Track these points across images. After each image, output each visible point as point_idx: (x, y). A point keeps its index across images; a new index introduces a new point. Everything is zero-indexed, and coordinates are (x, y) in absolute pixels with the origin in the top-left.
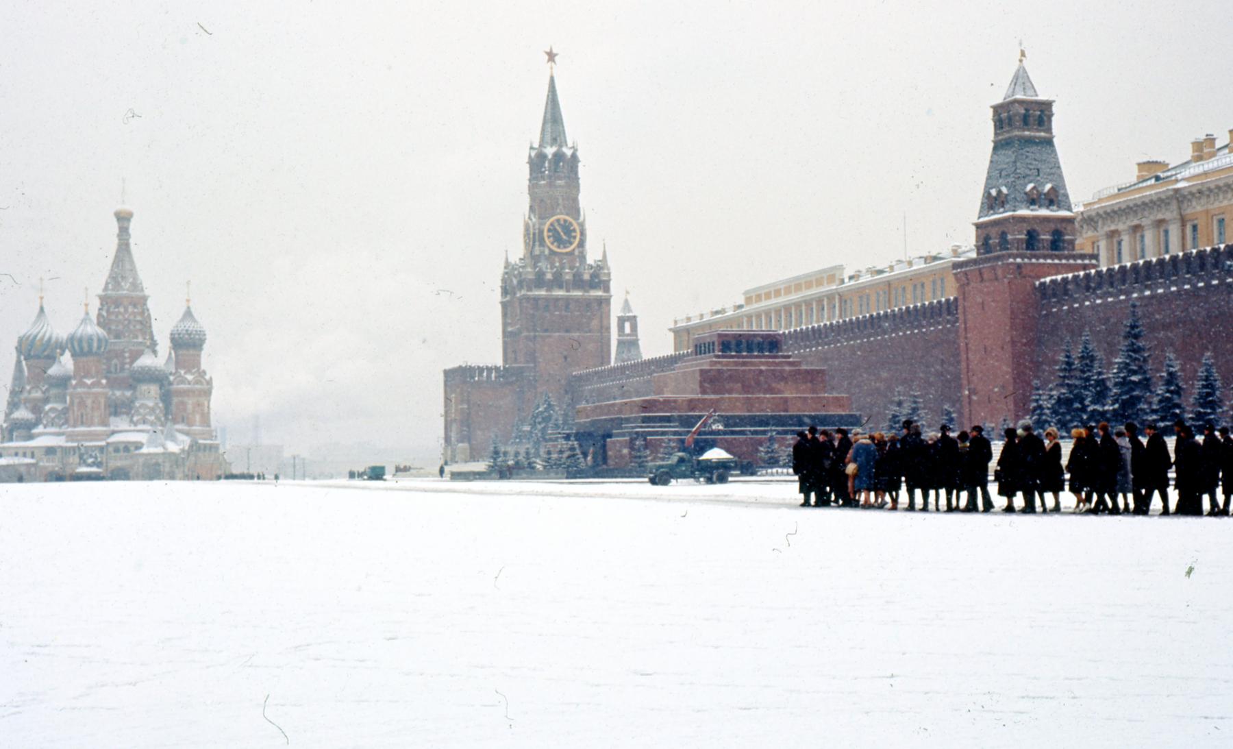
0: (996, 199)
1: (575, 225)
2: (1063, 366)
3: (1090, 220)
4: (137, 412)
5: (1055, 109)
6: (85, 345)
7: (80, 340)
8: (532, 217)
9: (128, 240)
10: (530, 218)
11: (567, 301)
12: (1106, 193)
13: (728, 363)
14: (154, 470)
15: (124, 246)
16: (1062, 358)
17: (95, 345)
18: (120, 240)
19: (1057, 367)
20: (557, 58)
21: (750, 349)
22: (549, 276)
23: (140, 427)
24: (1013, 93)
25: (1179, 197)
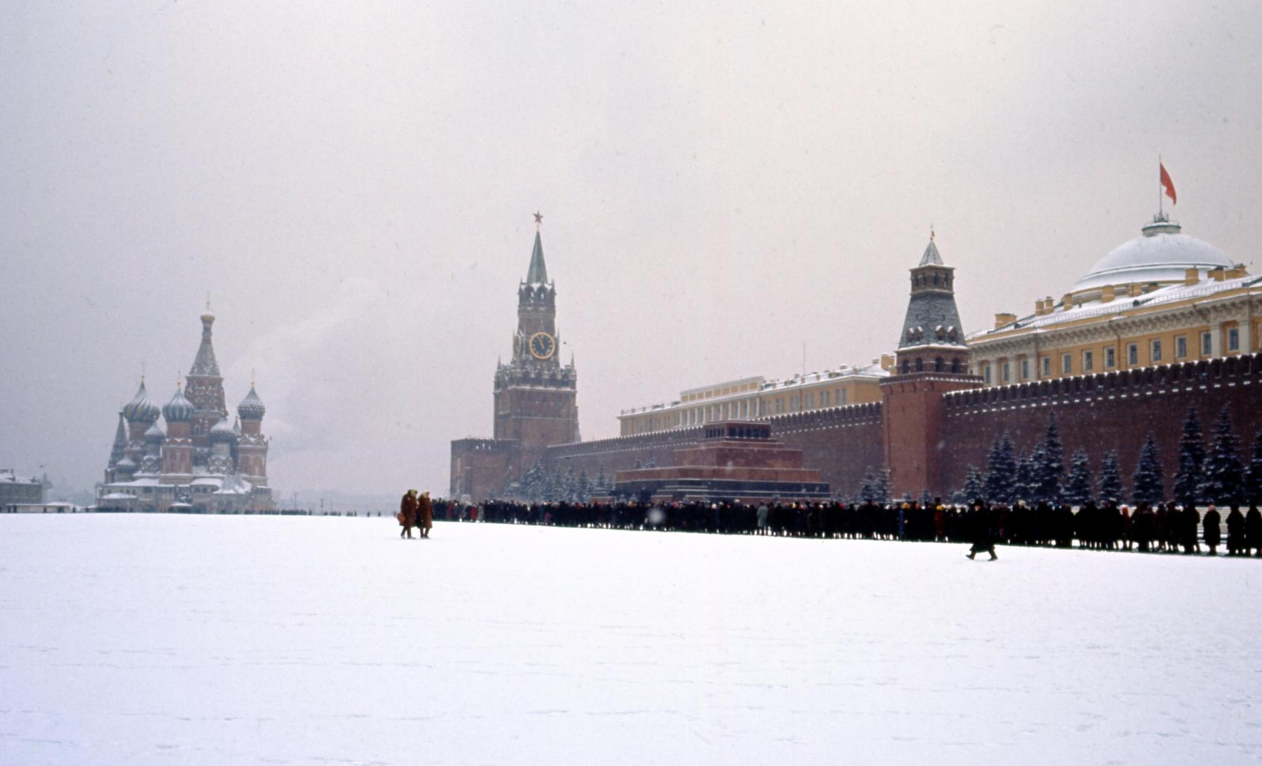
0: (913, 335)
1: (553, 340)
2: (994, 455)
5: (955, 273)
6: (177, 414)
7: (174, 409)
8: (521, 333)
10: (518, 333)
13: (735, 443)
14: (227, 507)
15: (207, 340)
16: (992, 449)
17: (185, 413)
19: (989, 456)
20: (542, 220)
22: (533, 376)
23: (215, 475)
24: (927, 262)
25: (1037, 339)
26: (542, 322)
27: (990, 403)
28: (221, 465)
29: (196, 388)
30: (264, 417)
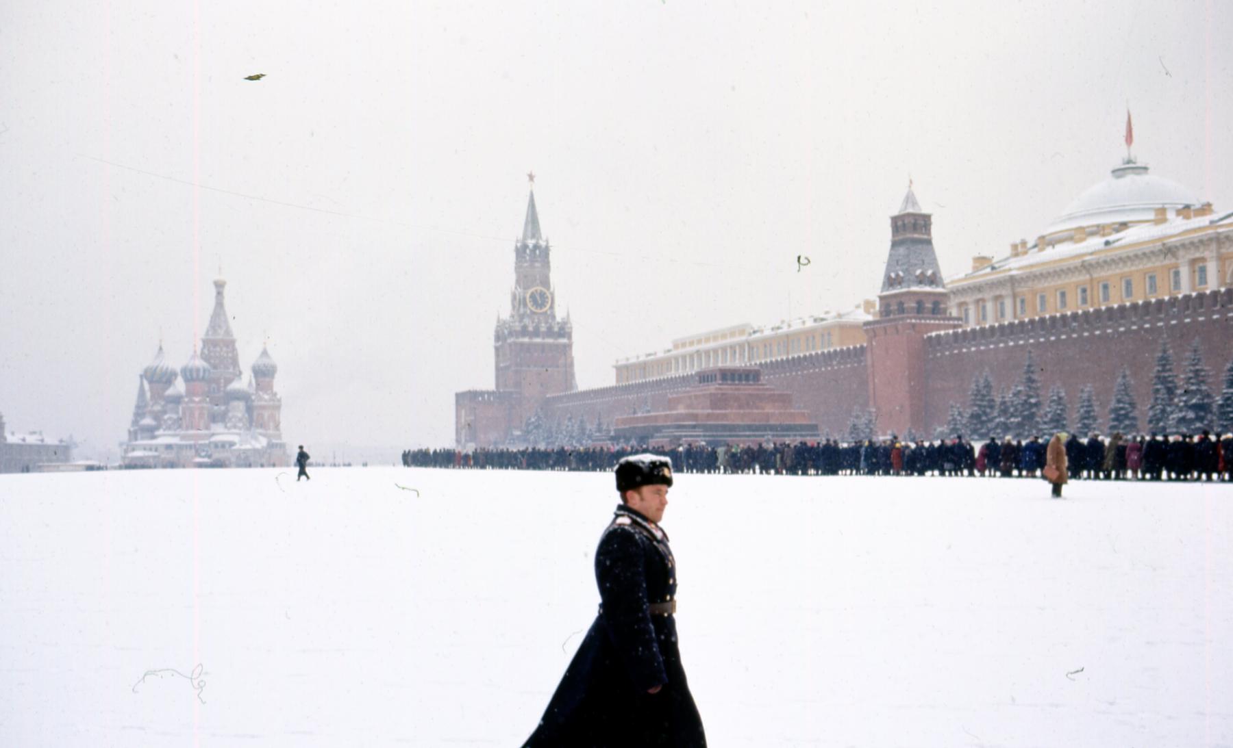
0: (894, 279)
1: (550, 296)
3: (957, 292)
4: (230, 419)
5: (933, 219)
7: (191, 371)
8: (518, 287)
10: (516, 288)
12: (956, 277)
13: (728, 388)
14: (246, 461)
15: (220, 304)
16: (973, 386)
17: (201, 374)
20: (535, 179)
22: (531, 329)
24: (906, 208)
25: (1012, 280)
26: (538, 277)
27: (969, 343)
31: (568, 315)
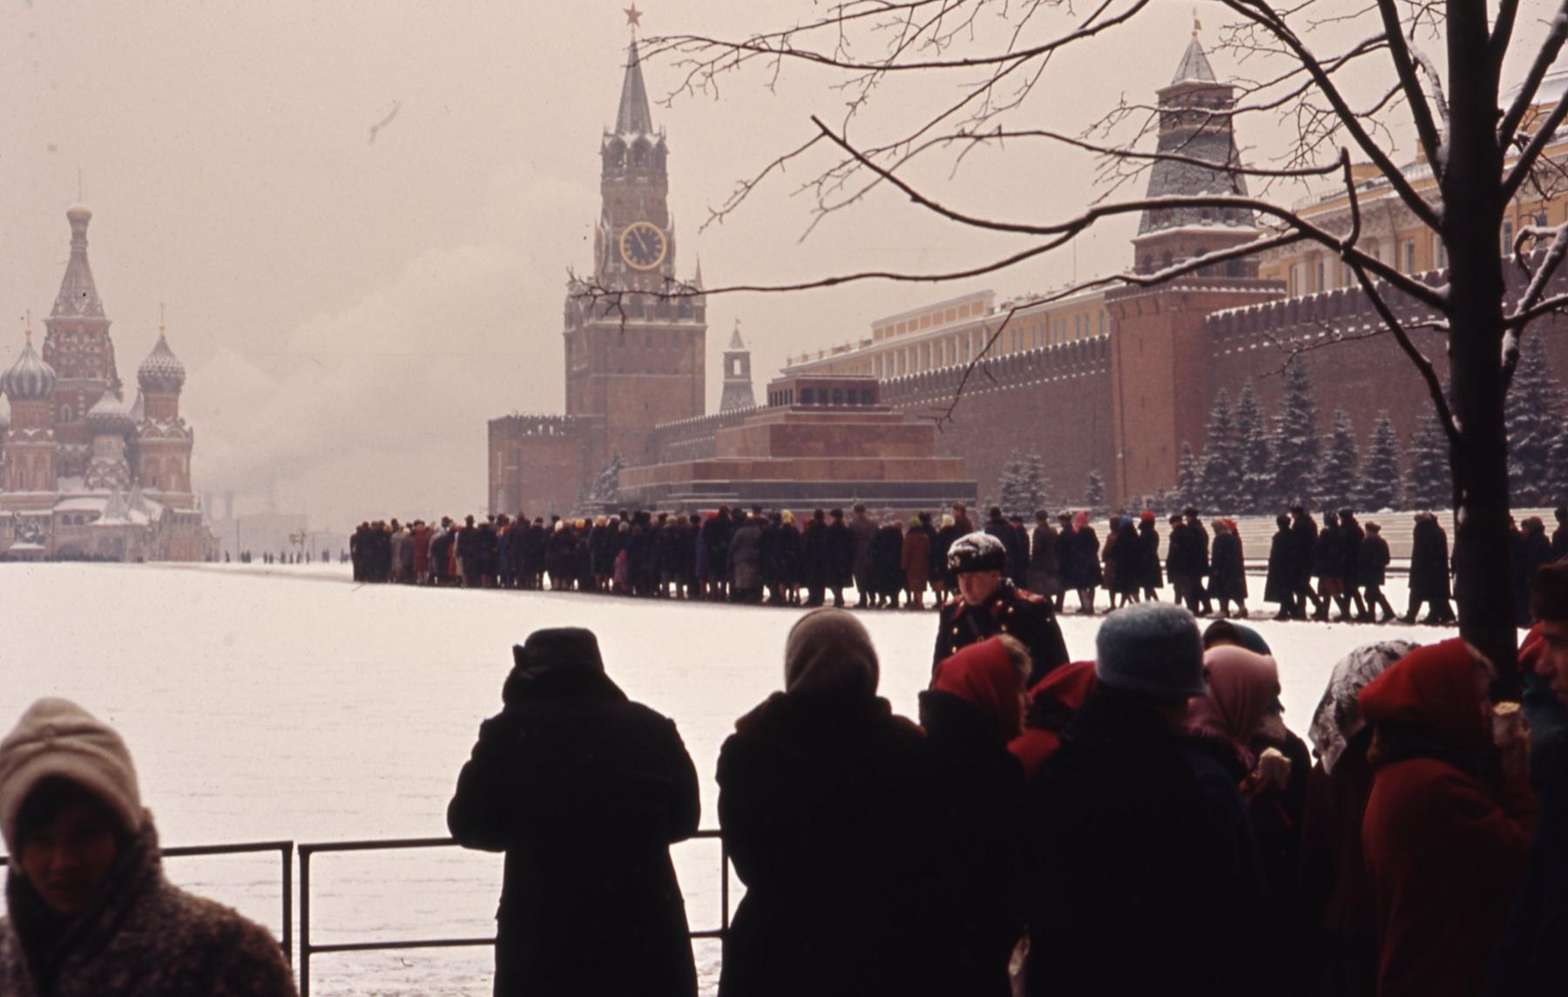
2: (1216, 425)
4: (94, 470)
6: (26, 385)
7: (20, 379)
8: (605, 224)
9: (84, 249)
10: (602, 225)
11: (649, 330)
13: (811, 416)
14: (112, 550)
17: (39, 385)
18: (73, 248)
19: (1209, 426)
20: (640, 19)
21: (837, 400)
23: (98, 491)
26: (642, 203)
27: (1274, 331)
28: (106, 475)
29: (62, 339)
30: (183, 388)
31: (698, 274)
